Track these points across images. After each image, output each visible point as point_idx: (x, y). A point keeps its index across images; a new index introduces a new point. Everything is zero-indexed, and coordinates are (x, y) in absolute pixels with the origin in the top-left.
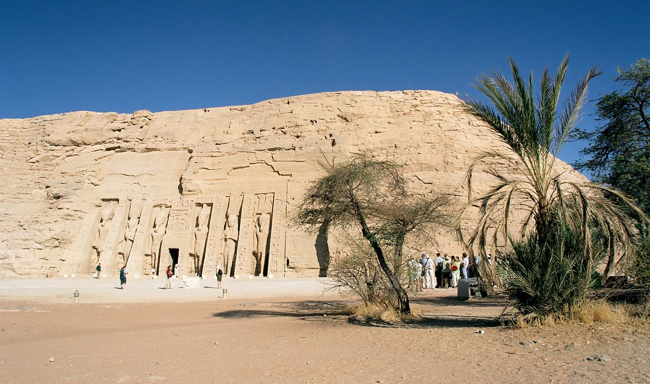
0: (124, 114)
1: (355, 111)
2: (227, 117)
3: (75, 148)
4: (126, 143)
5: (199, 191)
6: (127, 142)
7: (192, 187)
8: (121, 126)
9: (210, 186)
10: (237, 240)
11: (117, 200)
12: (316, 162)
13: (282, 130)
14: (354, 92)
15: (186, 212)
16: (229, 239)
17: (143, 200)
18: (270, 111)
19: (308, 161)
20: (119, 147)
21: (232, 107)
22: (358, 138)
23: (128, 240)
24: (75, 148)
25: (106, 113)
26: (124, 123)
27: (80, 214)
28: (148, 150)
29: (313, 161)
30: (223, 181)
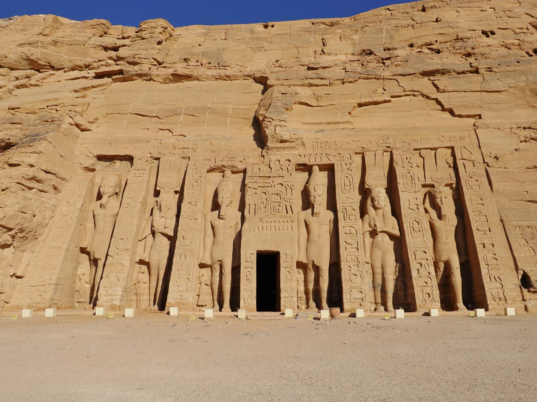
0: (121, 26)
3: (33, 75)
4: (132, 66)
5: (299, 142)
6: (135, 64)
7: (287, 133)
8: (120, 42)
9: (318, 134)
11: (130, 159)
12: (528, 92)
15: (280, 180)
16: (383, 232)
17: (184, 158)
18: (394, 22)
19: (511, 90)
20: (121, 72)
21: (314, 20)
23: (159, 237)
24: (33, 75)
26: (124, 38)
27: (55, 181)
28: (177, 77)
29: (523, 90)
30: (342, 126)
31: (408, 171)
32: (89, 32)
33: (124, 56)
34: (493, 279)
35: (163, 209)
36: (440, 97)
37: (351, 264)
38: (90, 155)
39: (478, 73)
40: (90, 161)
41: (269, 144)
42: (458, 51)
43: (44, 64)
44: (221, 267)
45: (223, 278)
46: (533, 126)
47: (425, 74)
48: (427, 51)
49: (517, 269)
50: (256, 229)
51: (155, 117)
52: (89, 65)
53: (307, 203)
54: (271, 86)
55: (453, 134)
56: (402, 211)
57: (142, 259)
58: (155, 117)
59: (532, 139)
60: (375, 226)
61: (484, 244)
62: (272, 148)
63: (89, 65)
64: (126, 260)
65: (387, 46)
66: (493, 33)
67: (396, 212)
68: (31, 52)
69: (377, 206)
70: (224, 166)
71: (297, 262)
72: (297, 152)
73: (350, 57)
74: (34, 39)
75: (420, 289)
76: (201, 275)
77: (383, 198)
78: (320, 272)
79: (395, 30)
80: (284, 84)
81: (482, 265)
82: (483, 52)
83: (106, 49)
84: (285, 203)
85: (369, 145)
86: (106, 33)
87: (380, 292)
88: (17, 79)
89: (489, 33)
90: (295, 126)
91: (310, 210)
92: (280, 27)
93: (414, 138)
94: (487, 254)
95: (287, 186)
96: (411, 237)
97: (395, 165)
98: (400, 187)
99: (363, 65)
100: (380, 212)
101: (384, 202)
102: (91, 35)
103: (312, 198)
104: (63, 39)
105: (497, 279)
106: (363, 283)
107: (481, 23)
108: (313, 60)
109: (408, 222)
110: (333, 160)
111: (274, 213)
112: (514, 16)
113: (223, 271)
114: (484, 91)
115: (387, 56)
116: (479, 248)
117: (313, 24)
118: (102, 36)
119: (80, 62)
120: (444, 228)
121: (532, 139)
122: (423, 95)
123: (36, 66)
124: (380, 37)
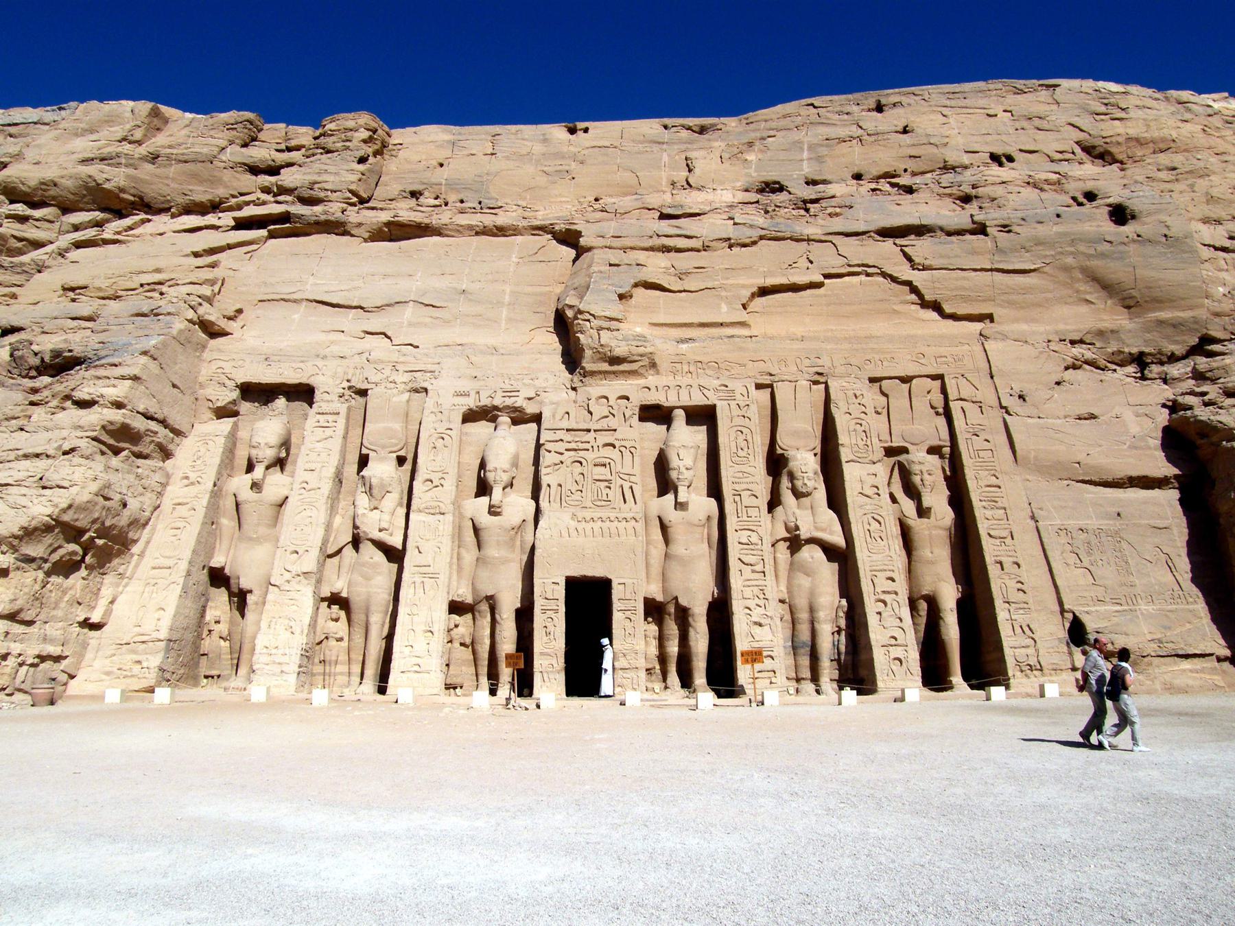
0: (283, 125)
1: (1134, 130)
2: (665, 146)
5: (646, 362)
8: (282, 158)
9: (684, 346)
13: (893, 180)
14: (1101, 84)
17: (416, 391)
19: (1047, 269)
20: (285, 217)
22: (1211, 199)
23: (368, 550)
24: (108, 221)
25: (223, 115)
26: (289, 149)
32: (221, 138)
33: (292, 185)
34: (1018, 630)
35: (375, 491)
36: (917, 277)
37: (751, 604)
38: (228, 382)
39: (986, 235)
40: (228, 395)
41: (588, 365)
42: (948, 191)
43: (132, 198)
44: (493, 610)
45: (497, 631)
46: (1088, 339)
47: (887, 233)
48: (887, 188)
49: (1063, 611)
50: (565, 534)
51: (356, 307)
52: (221, 203)
53: (665, 485)
54: (589, 249)
55: (942, 351)
56: (849, 500)
57: (335, 591)
58: (356, 307)
59: (1087, 362)
60: (797, 528)
61: (1001, 563)
62: (593, 374)
63: (221, 203)
64: (305, 597)
65: (811, 176)
66: (1010, 159)
67: (836, 501)
68: (105, 176)
69: (801, 490)
70: (496, 408)
71: (645, 599)
72: (642, 382)
73: (742, 196)
74: (112, 149)
76: (452, 626)
77: (811, 474)
78: (690, 619)
79: (827, 146)
80: (613, 245)
81: (998, 603)
82: (994, 196)
83: (254, 170)
84: (620, 482)
85: (783, 369)
86: (254, 139)
88: (76, 228)
89: (1004, 160)
90: (638, 330)
91: (670, 497)
92: (602, 131)
94: (1008, 582)
95: (623, 449)
96: (866, 551)
98: (845, 454)
99: (767, 212)
100: (805, 501)
102: (223, 143)
103: (673, 475)
104: (169, 151)
105: (1026, 629)
107: (989, 138)
108: (667, 198)
110: (712, 399)
111: (599, 503)
112: (1047, 127)
113: (497, 616)
114: (998, 270)
115: (813, 197)
116: (993, 571)
117: (666, 127)
118: (245, 145)
119: (201, 194)
121: (1087, 362)
122: (884, 275)
123: (115, 205)
124: (799, 158)
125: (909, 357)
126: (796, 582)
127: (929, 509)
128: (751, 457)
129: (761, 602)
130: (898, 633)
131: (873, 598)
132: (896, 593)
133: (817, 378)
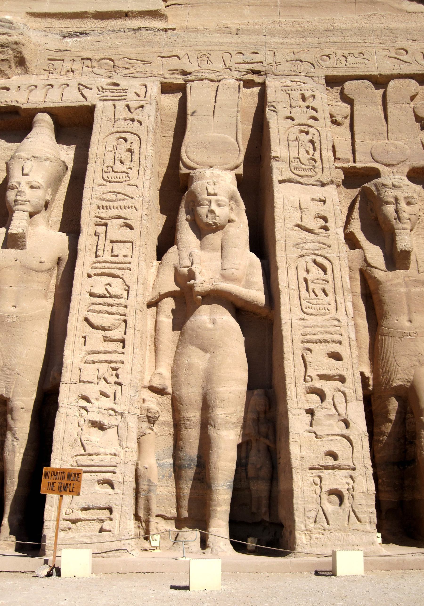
9: (69, 40)
10: (257, 294)
31: (305, 129)
37: (92, 391)
56: (279, 235)
60: (191, 275)
75: (311, 476)
77: (223, 198)
78: (9, 416)
85: (205, 66)
87: (190, 484)
91: (3, 230)
93: (327, 52)
97: (269, 113)
98: (278, 171)
100: (214, 239)
101: (226, 210)
103: (11, 195)
106: (122, 453)
109: (293, 266)
110: (92, 97)
120: (403, 290)
125: (386, 53)
126: (185, 360)
127: (407, 254)
128: (133, 173)
129: (110, 390)
130: (340, 447)
131: (302, 386)
132: (342, 379)
133: (250, 76)
